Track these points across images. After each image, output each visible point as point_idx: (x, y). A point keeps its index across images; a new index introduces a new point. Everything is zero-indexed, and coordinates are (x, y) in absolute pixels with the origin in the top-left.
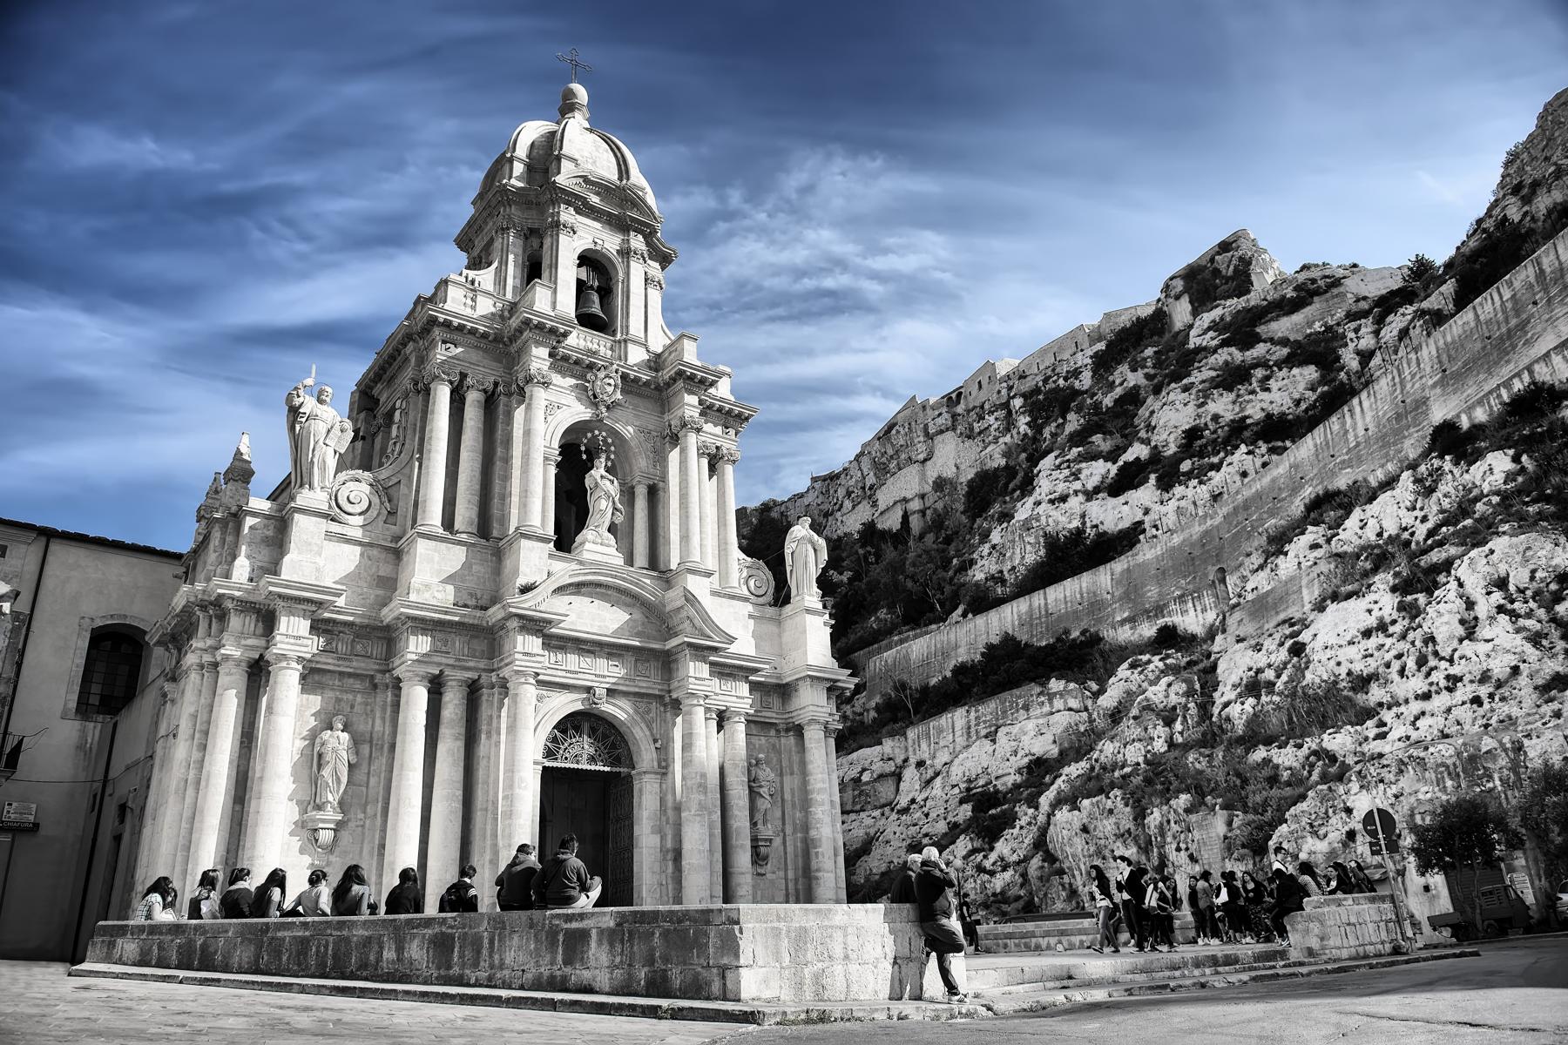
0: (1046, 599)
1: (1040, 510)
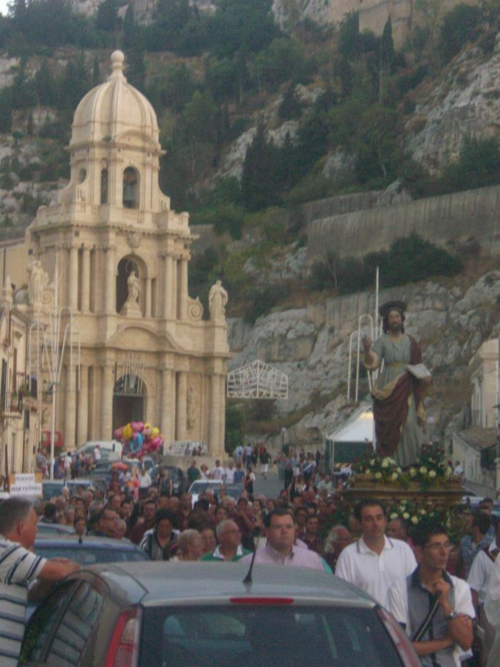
0: (450, 202)
1: (478, 101)
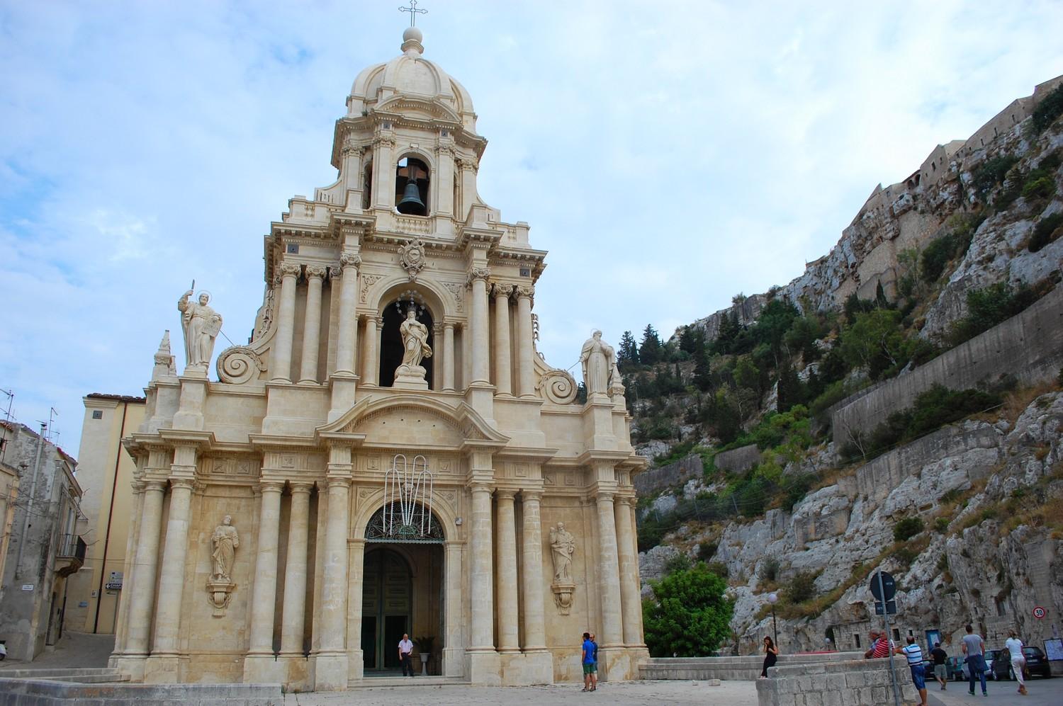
0: (969, 350)
1: (971, 272)
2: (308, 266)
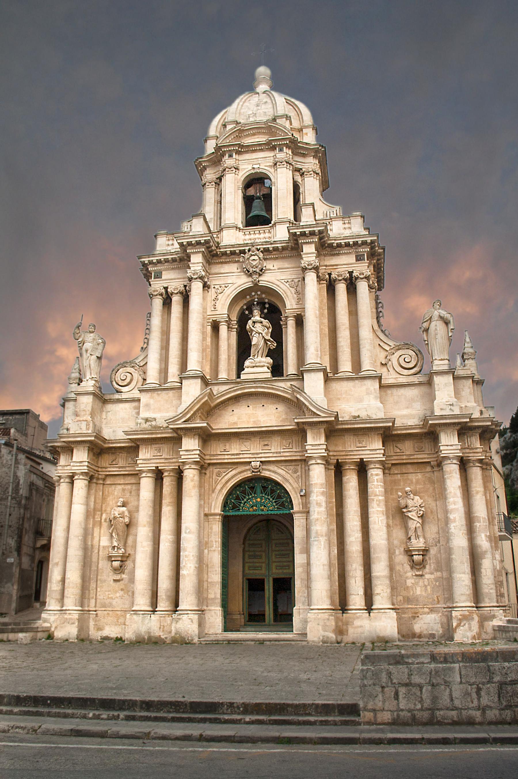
2: (169, 287)
